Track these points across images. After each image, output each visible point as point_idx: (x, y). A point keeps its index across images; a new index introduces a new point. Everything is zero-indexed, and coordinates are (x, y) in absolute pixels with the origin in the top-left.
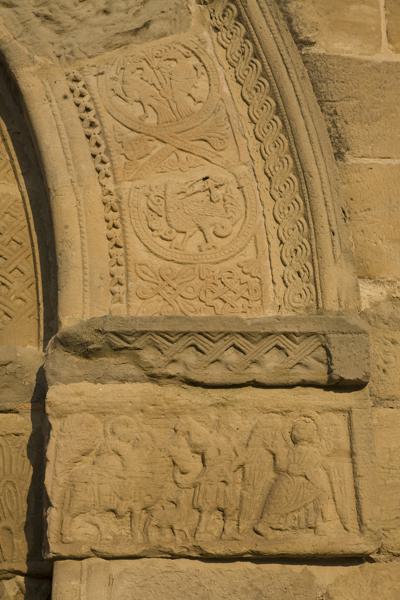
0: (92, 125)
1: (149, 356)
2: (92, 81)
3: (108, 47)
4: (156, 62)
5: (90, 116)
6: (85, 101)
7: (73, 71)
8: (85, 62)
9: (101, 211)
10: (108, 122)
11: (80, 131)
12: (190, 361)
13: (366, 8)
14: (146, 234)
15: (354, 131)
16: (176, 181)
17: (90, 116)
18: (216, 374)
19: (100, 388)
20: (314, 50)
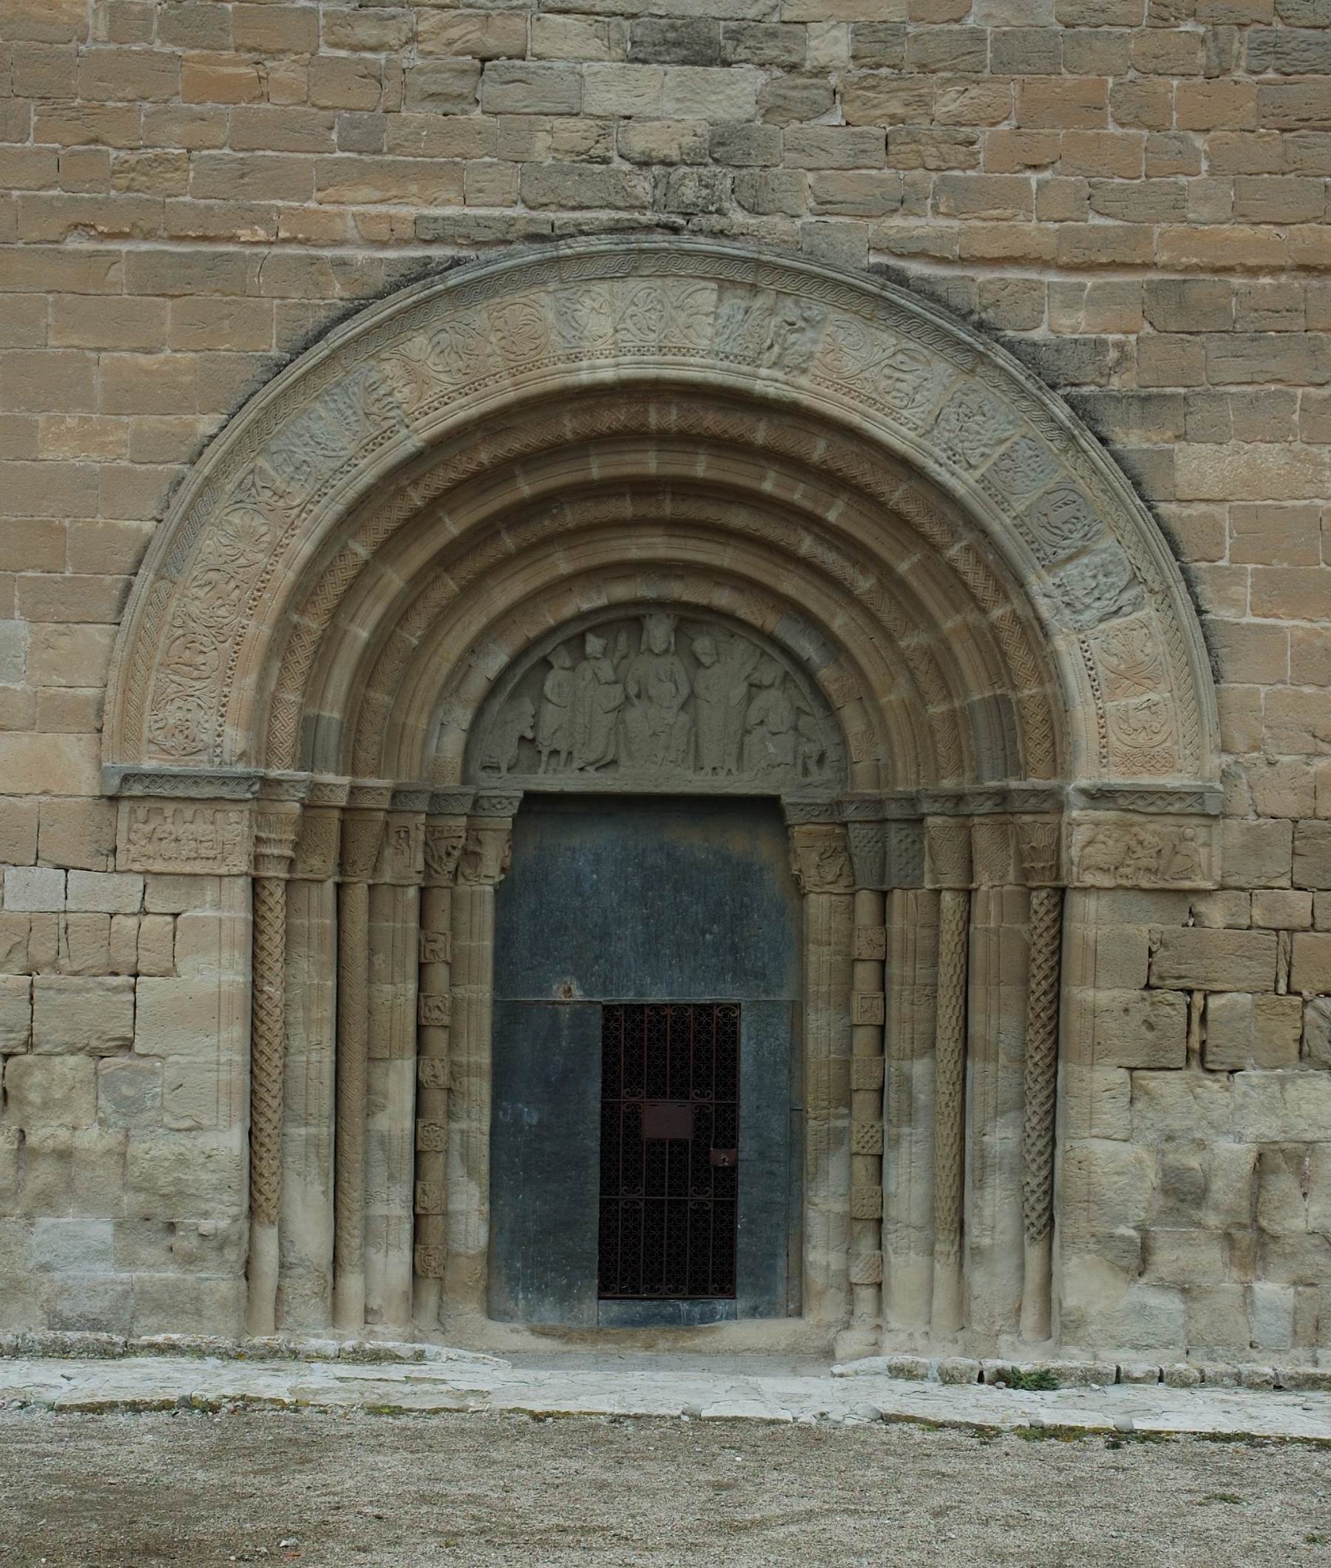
0: (1092, 669)
1: (1121, 801)
2: (1092, 642)
3: (1100, 621)
4: (1126, 632)
5: (1090, 664)
6: (1087, 655)
7: (1082, 637)
8: (1088, 632)
9: (1095, 719)
10: (1100, 668)
11: (1085, 672)
12: (1140, 805)
13: (1241, 589)
14: (1118, 732)
15: (1227, 668)
16: (1134, 701)
17: (1090, 664)
18: (1152, 809)
19: (1097, 813)
20: (1209, 616)
